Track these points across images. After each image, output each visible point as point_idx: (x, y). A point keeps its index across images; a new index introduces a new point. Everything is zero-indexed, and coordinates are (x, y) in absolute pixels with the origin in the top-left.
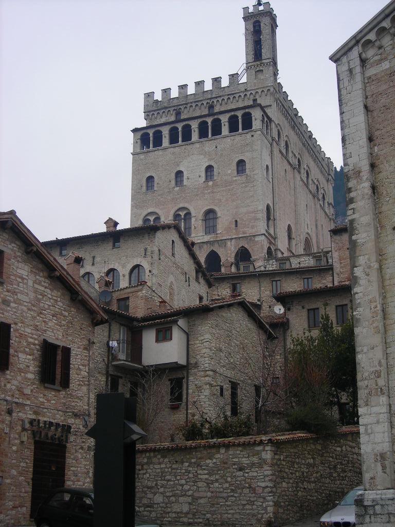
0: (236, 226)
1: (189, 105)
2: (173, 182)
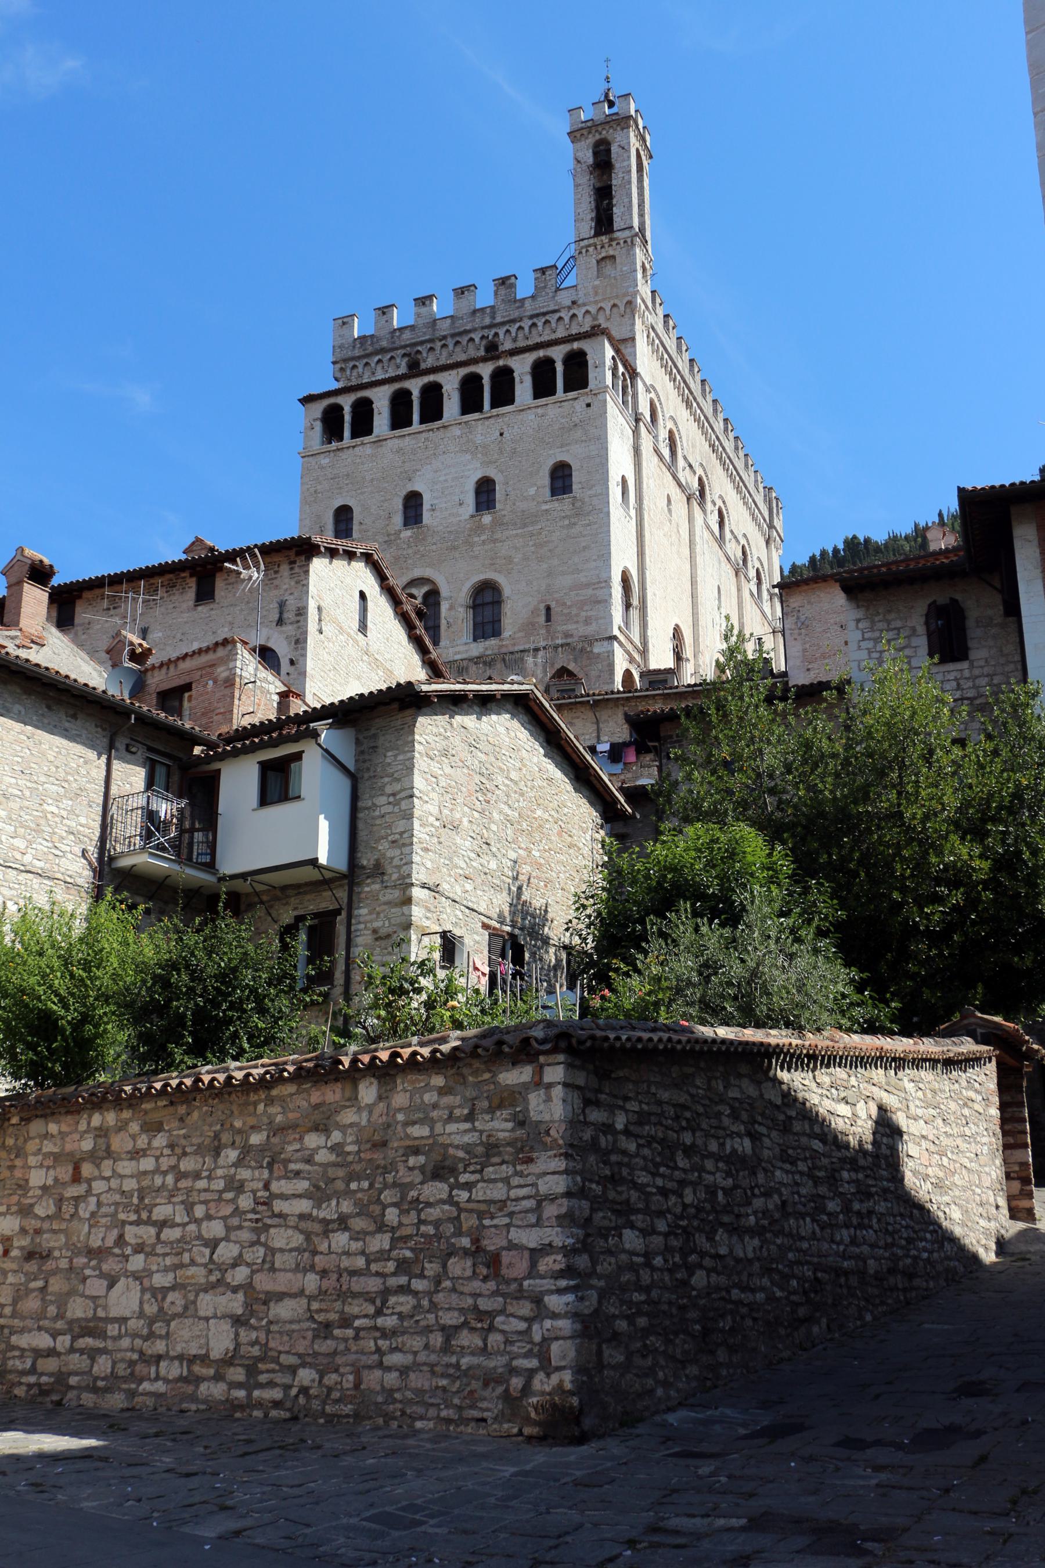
0: (548, 619)
2: (398, 519)
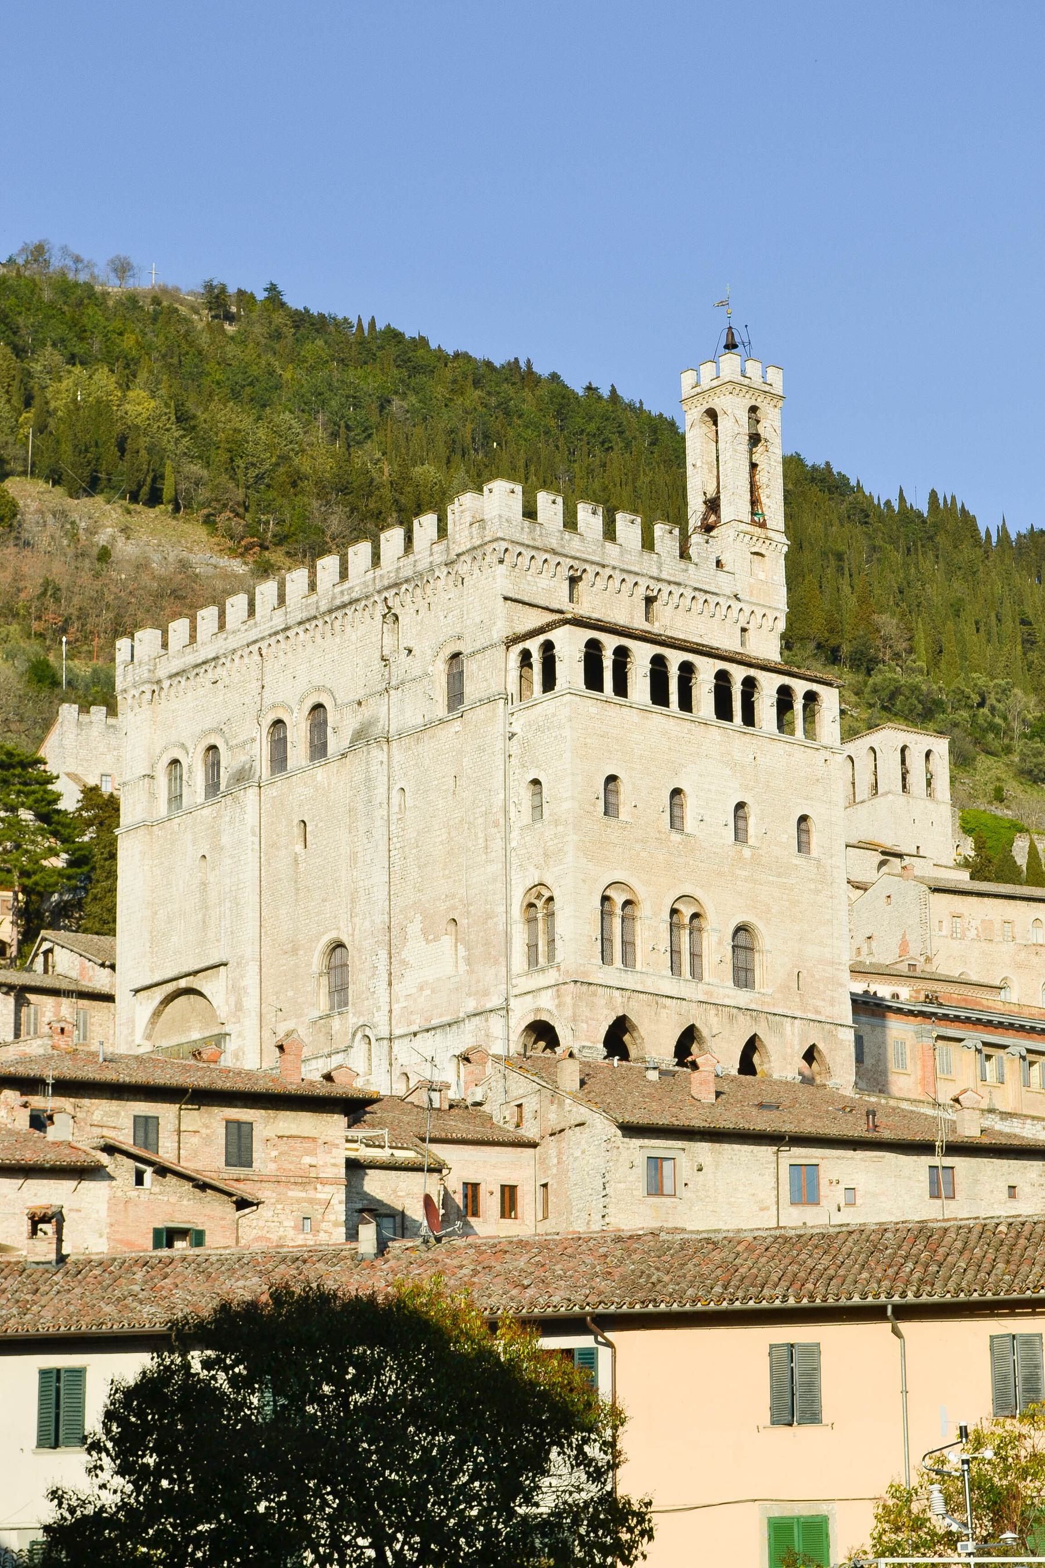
1: (608, 572)
